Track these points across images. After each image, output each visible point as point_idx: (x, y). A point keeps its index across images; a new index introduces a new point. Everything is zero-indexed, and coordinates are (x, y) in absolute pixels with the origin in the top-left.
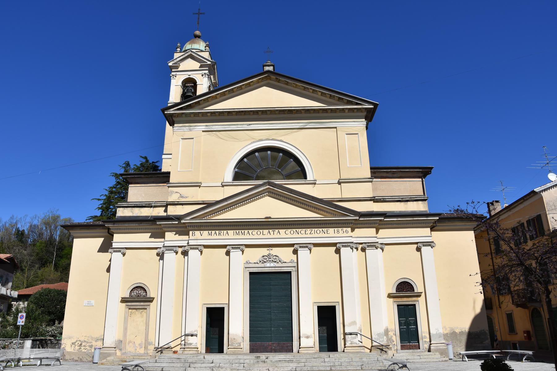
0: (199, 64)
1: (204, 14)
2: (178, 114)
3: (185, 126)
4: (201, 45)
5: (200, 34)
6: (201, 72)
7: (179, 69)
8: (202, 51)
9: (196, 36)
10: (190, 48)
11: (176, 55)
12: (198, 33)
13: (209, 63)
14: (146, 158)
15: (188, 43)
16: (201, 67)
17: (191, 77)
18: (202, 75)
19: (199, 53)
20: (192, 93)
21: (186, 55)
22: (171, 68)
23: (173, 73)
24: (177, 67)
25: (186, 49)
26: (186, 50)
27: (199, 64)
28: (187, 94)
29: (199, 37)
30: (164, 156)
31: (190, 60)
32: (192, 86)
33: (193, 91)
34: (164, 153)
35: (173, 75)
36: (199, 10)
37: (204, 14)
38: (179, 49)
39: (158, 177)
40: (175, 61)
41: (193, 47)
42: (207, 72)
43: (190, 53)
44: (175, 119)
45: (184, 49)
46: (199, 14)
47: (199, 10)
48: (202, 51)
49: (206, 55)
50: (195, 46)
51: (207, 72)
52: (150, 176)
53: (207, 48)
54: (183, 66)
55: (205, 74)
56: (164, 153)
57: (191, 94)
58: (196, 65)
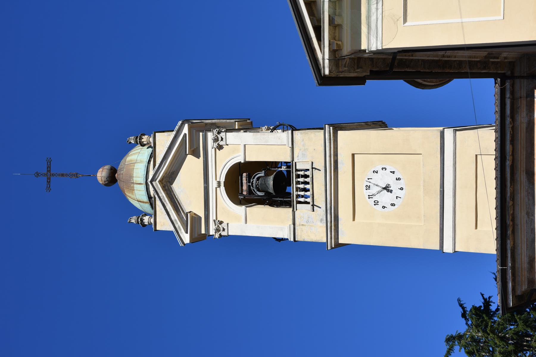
0: (190, 158)
1: (49, 188)
2: (332, 38)
3: (369, 17)
4: (137, 161)
5: (107, 167)
6: (211, 152)
7: (202, 214)
8: (153, 156)
9: (112, 179)
10: (143, 187)
11: (163, 224)
12: (102, 174)
13: (186, 130)
14: (450, 339)
15: (128, 194)
16: (195, 153)
17: (223, 180)
18: (220, 147)
19: (159, 160)
20: (267, 175)
21: (162, 194)
22: (198, 238)
23: (212, 232)
24: (196, 219)
25: (145, 199)
26: (150, 197)
27: (190, 158)
28: (271, 190)
29: (113, 172)
30: (448, 248)
31: (177, 186)
32: (249, 178)
33: (262, 174)
34: (437, 248)
35: (217, 230)
36: (37, 174)
37: (49, 188)
38: (146, 219)
39: (513, 198)
40: (178, 224)
41: (142, 180)
42: (210, 136)
43: (157, 183)
44: (346, 50)
45: (147, 208)
46: (49, 174)
47: (37, 174)
48: (153, 156)
49: (163, 140)
50: (139, 173)
51: (210, 136)
52: (509, 222)
53: (145, 139)
54: (192, 201)
55: (216, 140)
56: (437, 248)
57: (270, 181)
58: (192, 165)
